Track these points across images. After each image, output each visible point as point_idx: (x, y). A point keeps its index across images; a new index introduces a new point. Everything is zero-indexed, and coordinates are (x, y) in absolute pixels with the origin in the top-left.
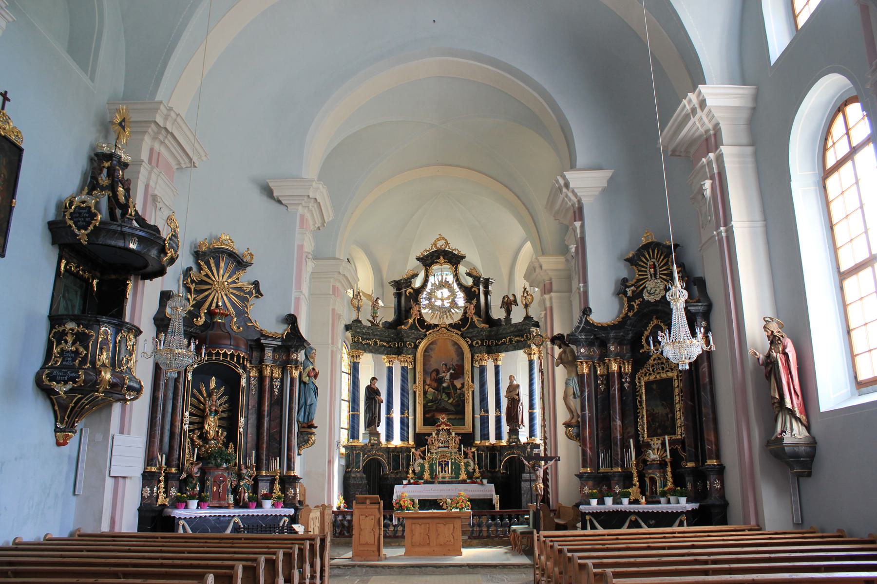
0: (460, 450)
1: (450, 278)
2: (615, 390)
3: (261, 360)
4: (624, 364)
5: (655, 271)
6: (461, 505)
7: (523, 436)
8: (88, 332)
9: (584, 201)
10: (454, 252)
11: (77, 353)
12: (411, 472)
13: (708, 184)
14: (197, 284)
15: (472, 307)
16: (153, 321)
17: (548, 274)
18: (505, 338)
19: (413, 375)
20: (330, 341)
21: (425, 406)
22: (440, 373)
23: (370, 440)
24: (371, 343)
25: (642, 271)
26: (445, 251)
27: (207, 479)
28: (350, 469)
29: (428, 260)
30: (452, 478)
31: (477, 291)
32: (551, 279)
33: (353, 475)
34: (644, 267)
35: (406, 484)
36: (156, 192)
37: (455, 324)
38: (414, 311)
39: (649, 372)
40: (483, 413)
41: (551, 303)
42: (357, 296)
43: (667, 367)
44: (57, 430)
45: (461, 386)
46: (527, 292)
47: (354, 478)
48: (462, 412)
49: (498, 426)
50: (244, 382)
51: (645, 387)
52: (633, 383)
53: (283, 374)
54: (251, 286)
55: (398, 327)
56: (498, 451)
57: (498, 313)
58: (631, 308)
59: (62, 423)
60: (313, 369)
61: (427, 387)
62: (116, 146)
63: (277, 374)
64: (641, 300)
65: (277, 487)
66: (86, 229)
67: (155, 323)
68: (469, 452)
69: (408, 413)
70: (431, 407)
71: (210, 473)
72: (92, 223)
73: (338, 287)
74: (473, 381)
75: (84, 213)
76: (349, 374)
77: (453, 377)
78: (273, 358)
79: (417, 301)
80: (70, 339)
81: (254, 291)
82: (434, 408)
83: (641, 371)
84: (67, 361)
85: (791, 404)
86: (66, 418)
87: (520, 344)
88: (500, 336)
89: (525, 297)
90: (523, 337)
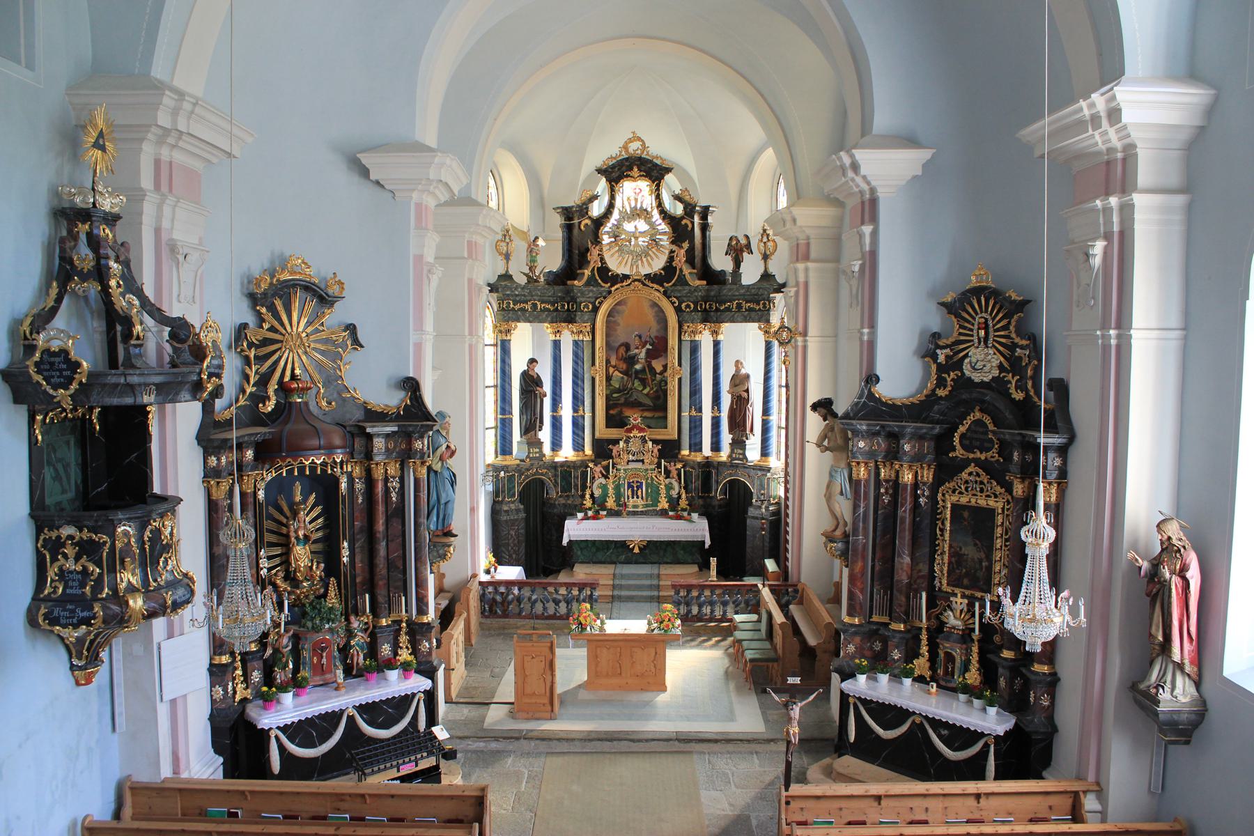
0: (659, 466)
1: (648, 201)
2: (905, 511)
3: (369, 455)
4: (922, 468)
5: (987, 334)
6: (668, 626)
7: (753, 453)
8: (97, 540)
9: (881, 193)
11: (85, 572)
12: (588, 496)
13: (1098, 247)
14: (257, 347)
15: (683, 252)
16: (196, 442)
17: (804, 231)
18: (730, 302)
19: (591, 351)
20: (467, 333)
21: (608, 398)
22: (632, 348)
23: (529, 453)
24: (528, 307)
25: (965, 328)
26: (640, 159)
27: (303, 648)
28: (500, 499)
29: (616, 173)
30: (647, 506)
31: (690, 226)
32: (808, 238)
33: (506, 508)
34: (968, 322)
35: (582, 520)
36: (175, 237)
37: (655, 275)
38: (593, 256)
40: (694, 413)
41: (807, 276)
42: (505, 236)
43: (988, 491)
44: (73, 668)
45: (662, 369)
46: (768, 235)
47: (507, 511)
48: (664, 408)
49: (715, 431)
50: (344, 486)
51: (951, 511)
52: (933, 499)
53: (402, 469)
54: (344, 334)
55: (569, 282)
56: (714, 468)
57: (720, 261)
58: (941, 383)
59: (80, 659)
60: (448, 447)
61: (611, 370)
62: (93, 189)
63: (393, 470)
65: (404, 639)
66: (66, 388)
67: (199, 444)
68: (672, 469)
69: (584, 410)
70: (618, 398)
71: (306, 639)
72: (74, 378)
73: (476, 242)
74: (680, 364)
75: (59, 363)
76: (495, 345)
77: (651, 355)
78: (387, 448)
79: (597, 241)
80: (70, 551)
81: (349, 343)
82: (622, 400)
83: (947, 484)
84: (72, 588)
85: (1179, 657)
86: (85, 653)
87: (753, 314)
88: (724, 297)
89: (765, 243)
90: (759, 305)
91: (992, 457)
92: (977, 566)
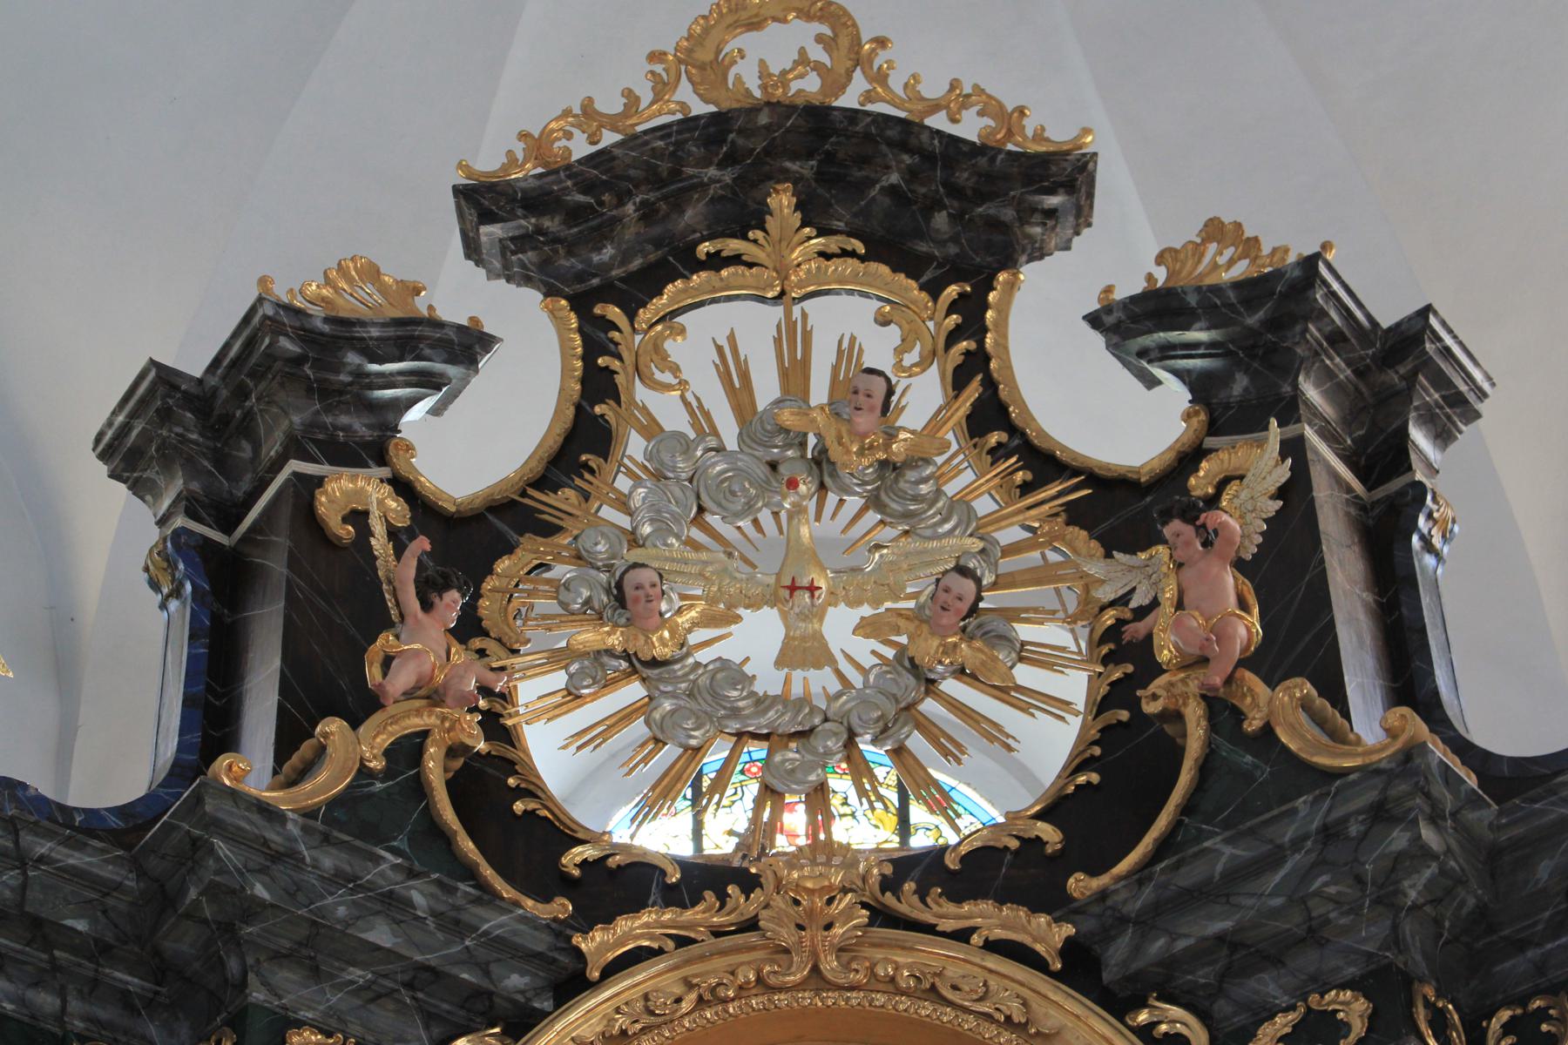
10: (938, 122)
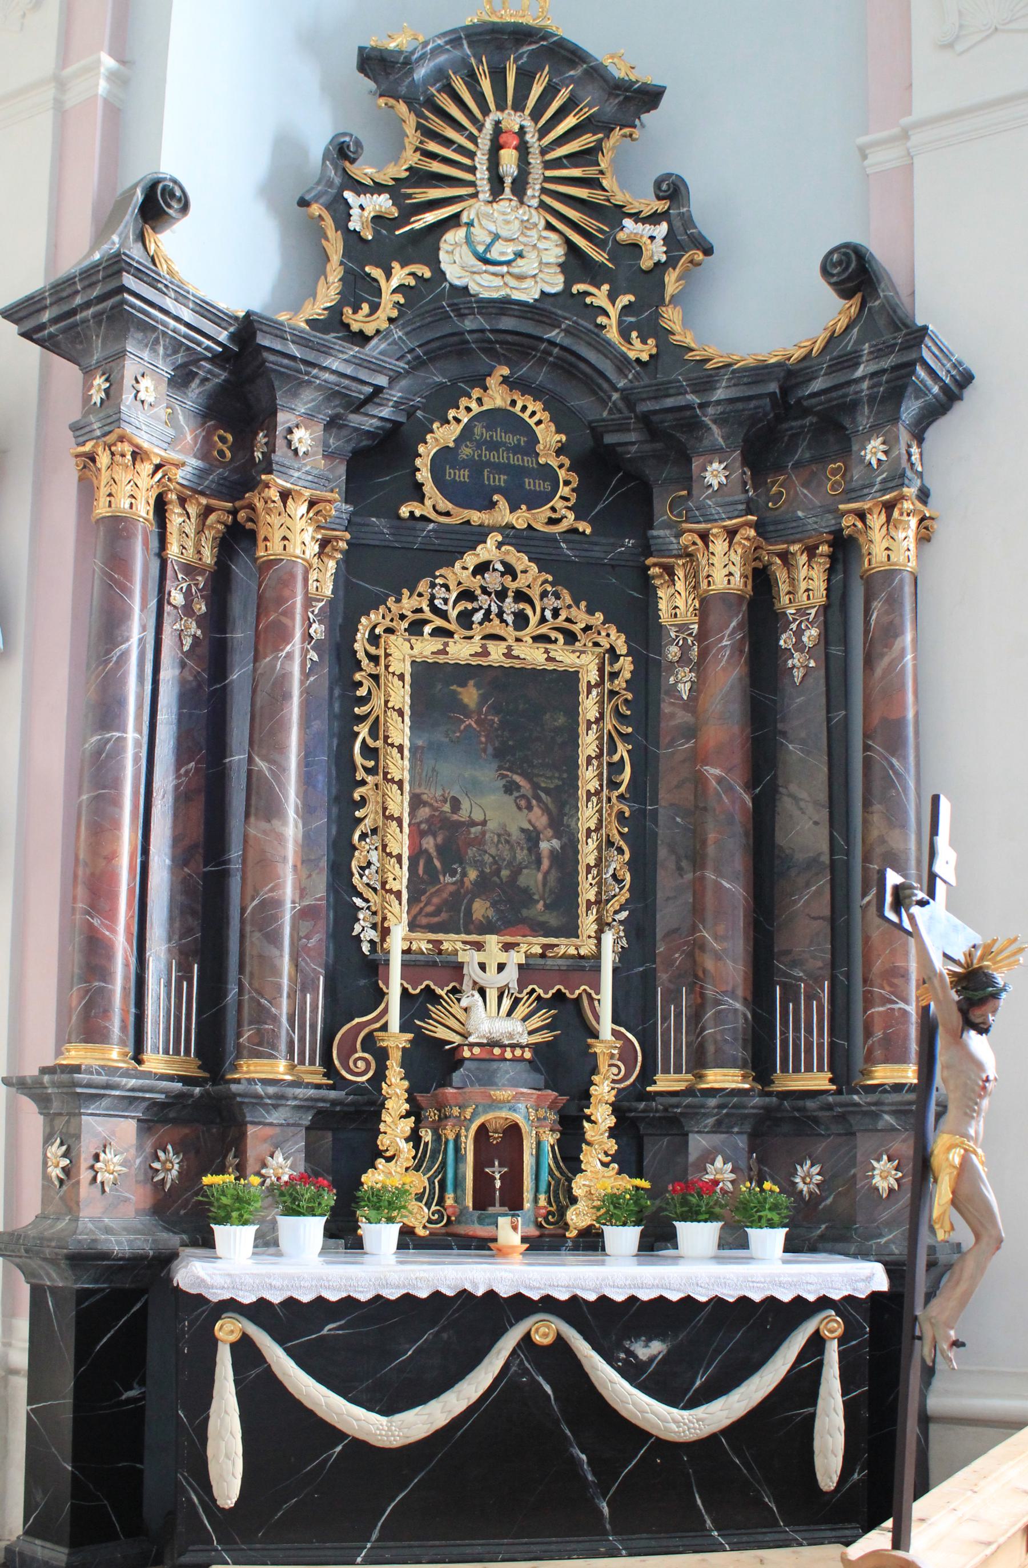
39: (439, 622)
43: (543, 620)
64: (428, 274)
91: (552, 521)
92: (521, 855)
